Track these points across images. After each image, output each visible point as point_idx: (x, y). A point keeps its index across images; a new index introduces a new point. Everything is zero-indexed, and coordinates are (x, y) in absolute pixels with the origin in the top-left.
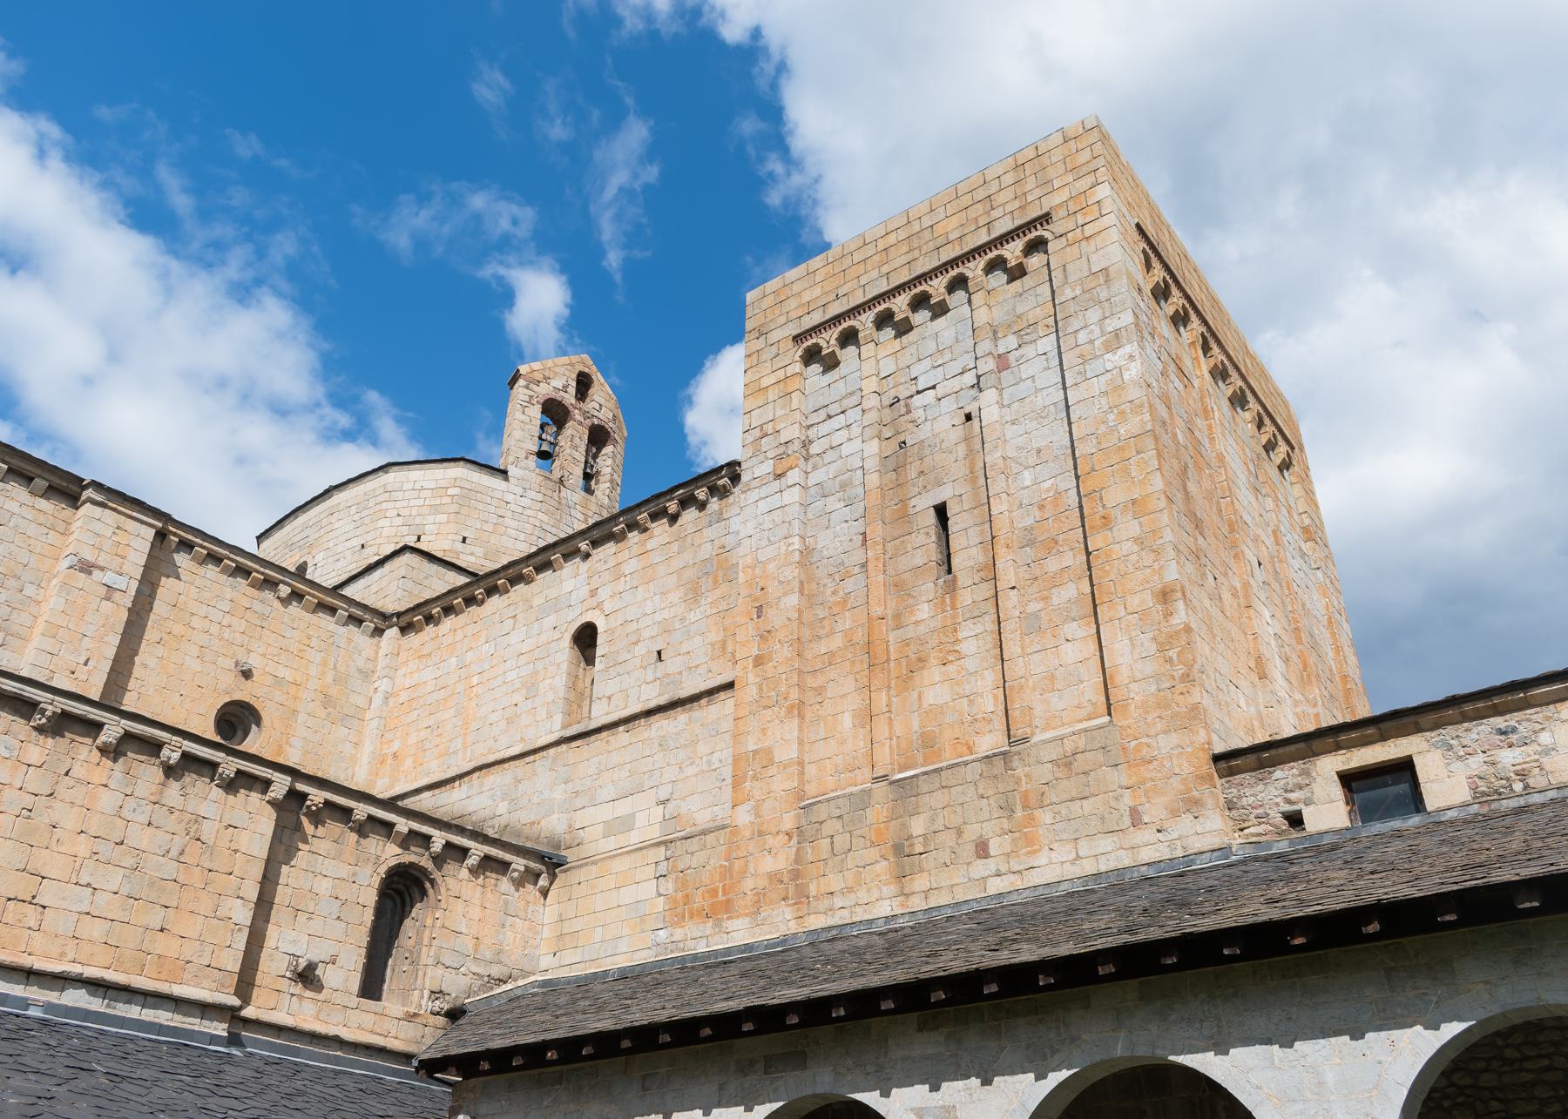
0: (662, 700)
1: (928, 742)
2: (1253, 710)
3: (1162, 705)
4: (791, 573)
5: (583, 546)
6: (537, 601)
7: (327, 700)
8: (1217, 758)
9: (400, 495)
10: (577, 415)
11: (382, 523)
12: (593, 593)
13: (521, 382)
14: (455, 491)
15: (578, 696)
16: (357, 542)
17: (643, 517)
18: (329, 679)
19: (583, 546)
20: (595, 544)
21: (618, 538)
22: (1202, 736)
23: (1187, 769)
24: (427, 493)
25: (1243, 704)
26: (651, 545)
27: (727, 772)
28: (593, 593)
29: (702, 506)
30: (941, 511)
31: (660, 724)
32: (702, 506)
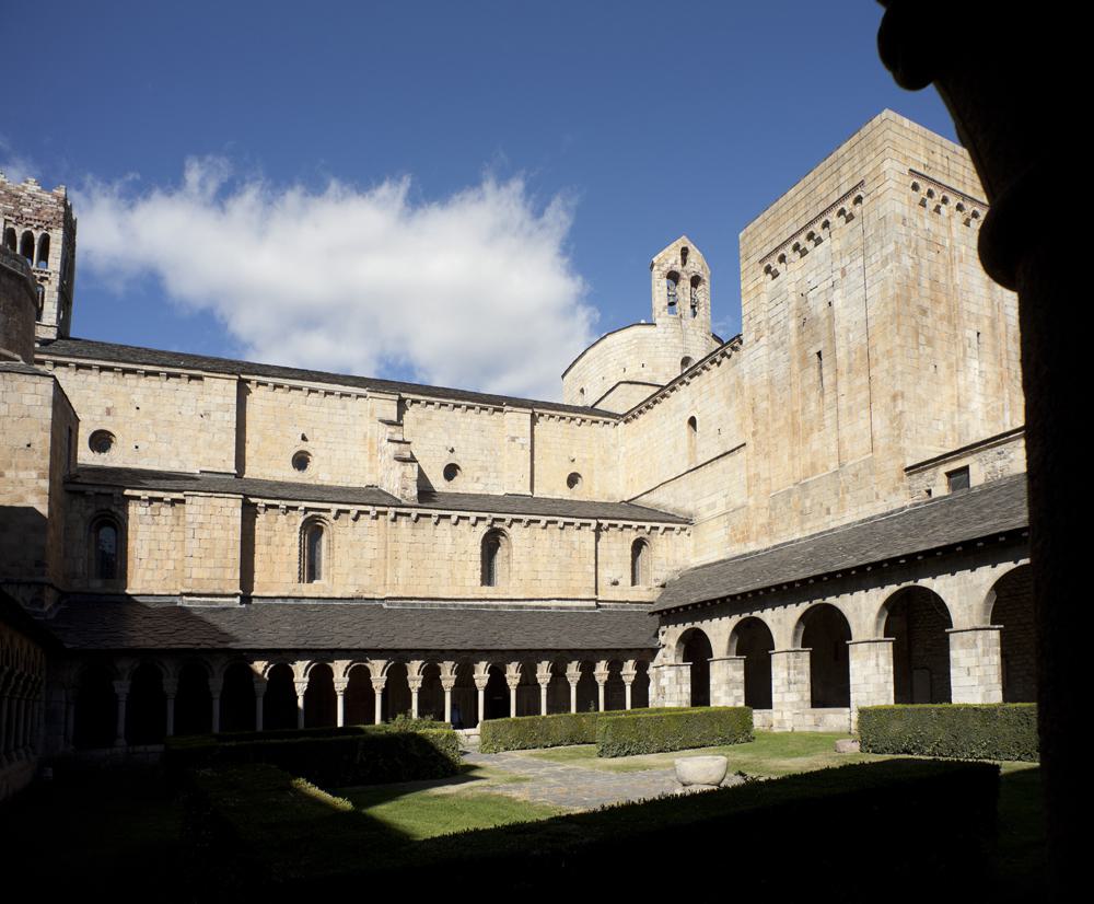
0: (721, 453)
1: (813, 467)
2: (948, 426)
3: (889, 449)
4: (764, 391)
5: (687, 379)
6: (673, 407)
7: (603, 462)
8: (906, 470)
9: (612, 349)
10: (684, 275)
11: (609, 365)
12: (693, 401)
13: (655, 268)
14: (635, 341)
15: (693, 449)
16: (601, 377)
17: (707, 364)
18: (602, 453)
19: (687, 379)
20: (691, 377)
21: (699, 374)
22: (902, 462)
23: (895, 476)
24: (624, 345)
25: (941, 427)
26: (712, 377)
27: (746, 483)
28: (693, 401)
29: (729, 357)
30: (819, 354)
31: (723, 462)
32: (729, 357)
